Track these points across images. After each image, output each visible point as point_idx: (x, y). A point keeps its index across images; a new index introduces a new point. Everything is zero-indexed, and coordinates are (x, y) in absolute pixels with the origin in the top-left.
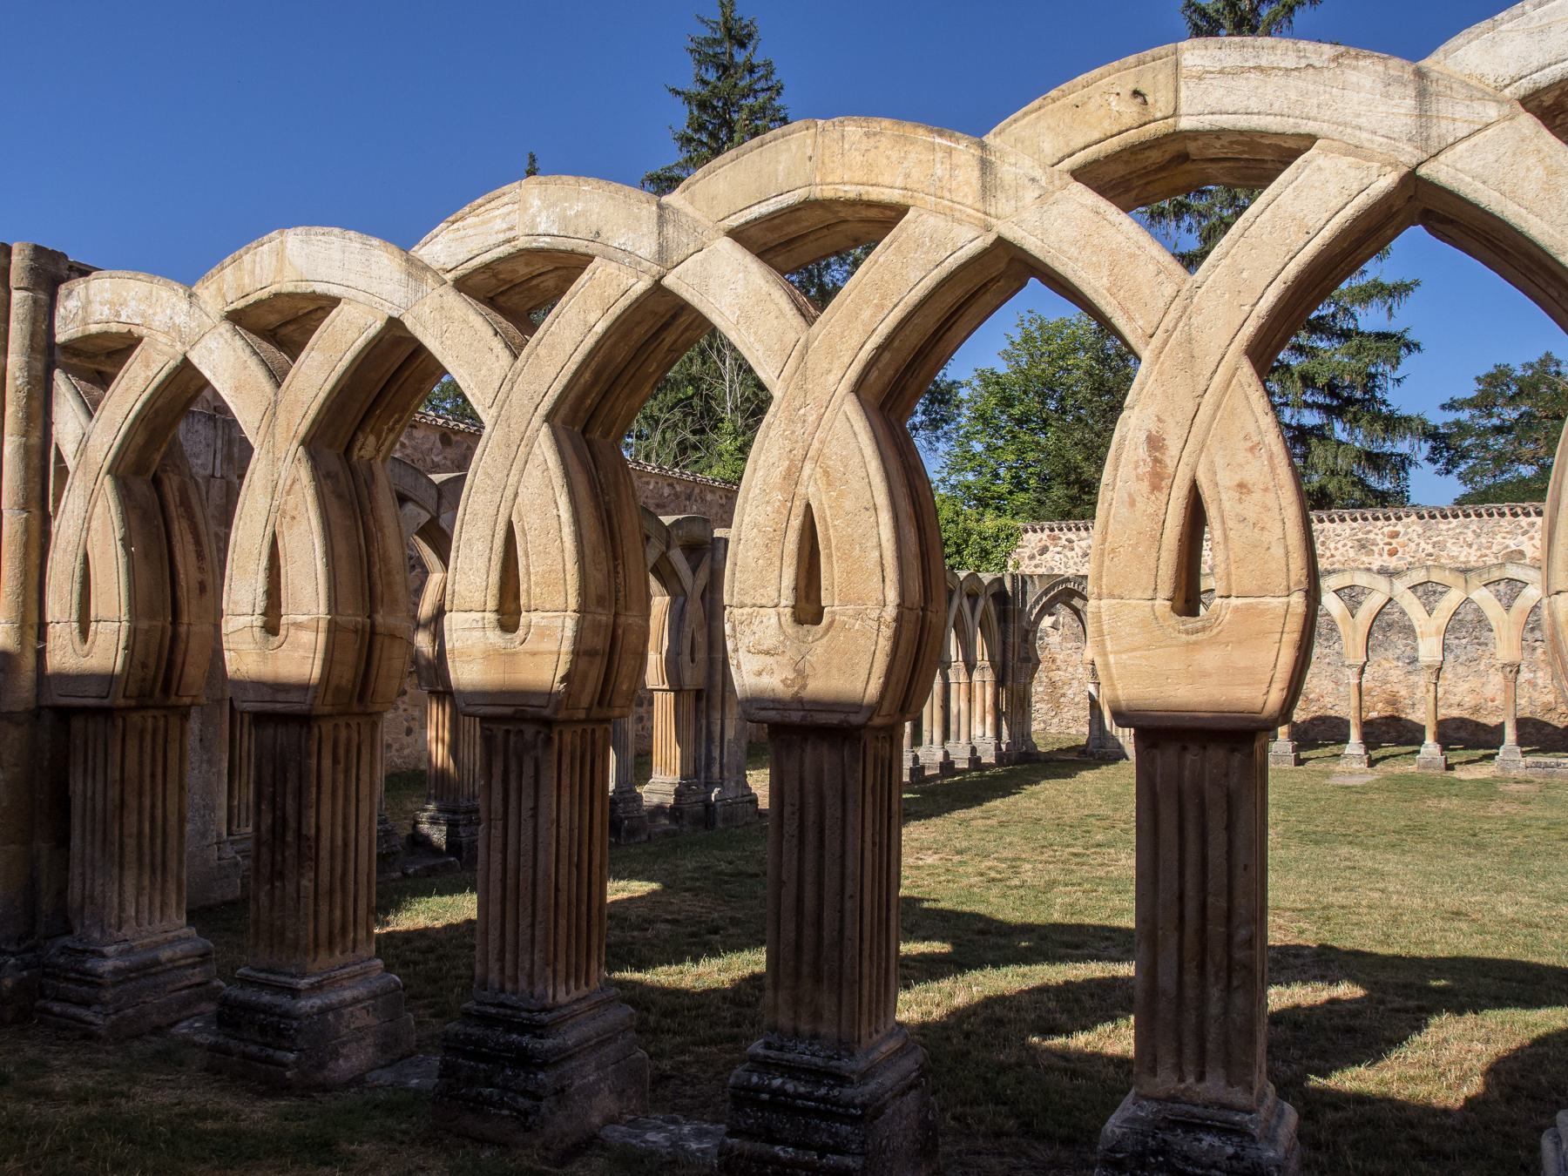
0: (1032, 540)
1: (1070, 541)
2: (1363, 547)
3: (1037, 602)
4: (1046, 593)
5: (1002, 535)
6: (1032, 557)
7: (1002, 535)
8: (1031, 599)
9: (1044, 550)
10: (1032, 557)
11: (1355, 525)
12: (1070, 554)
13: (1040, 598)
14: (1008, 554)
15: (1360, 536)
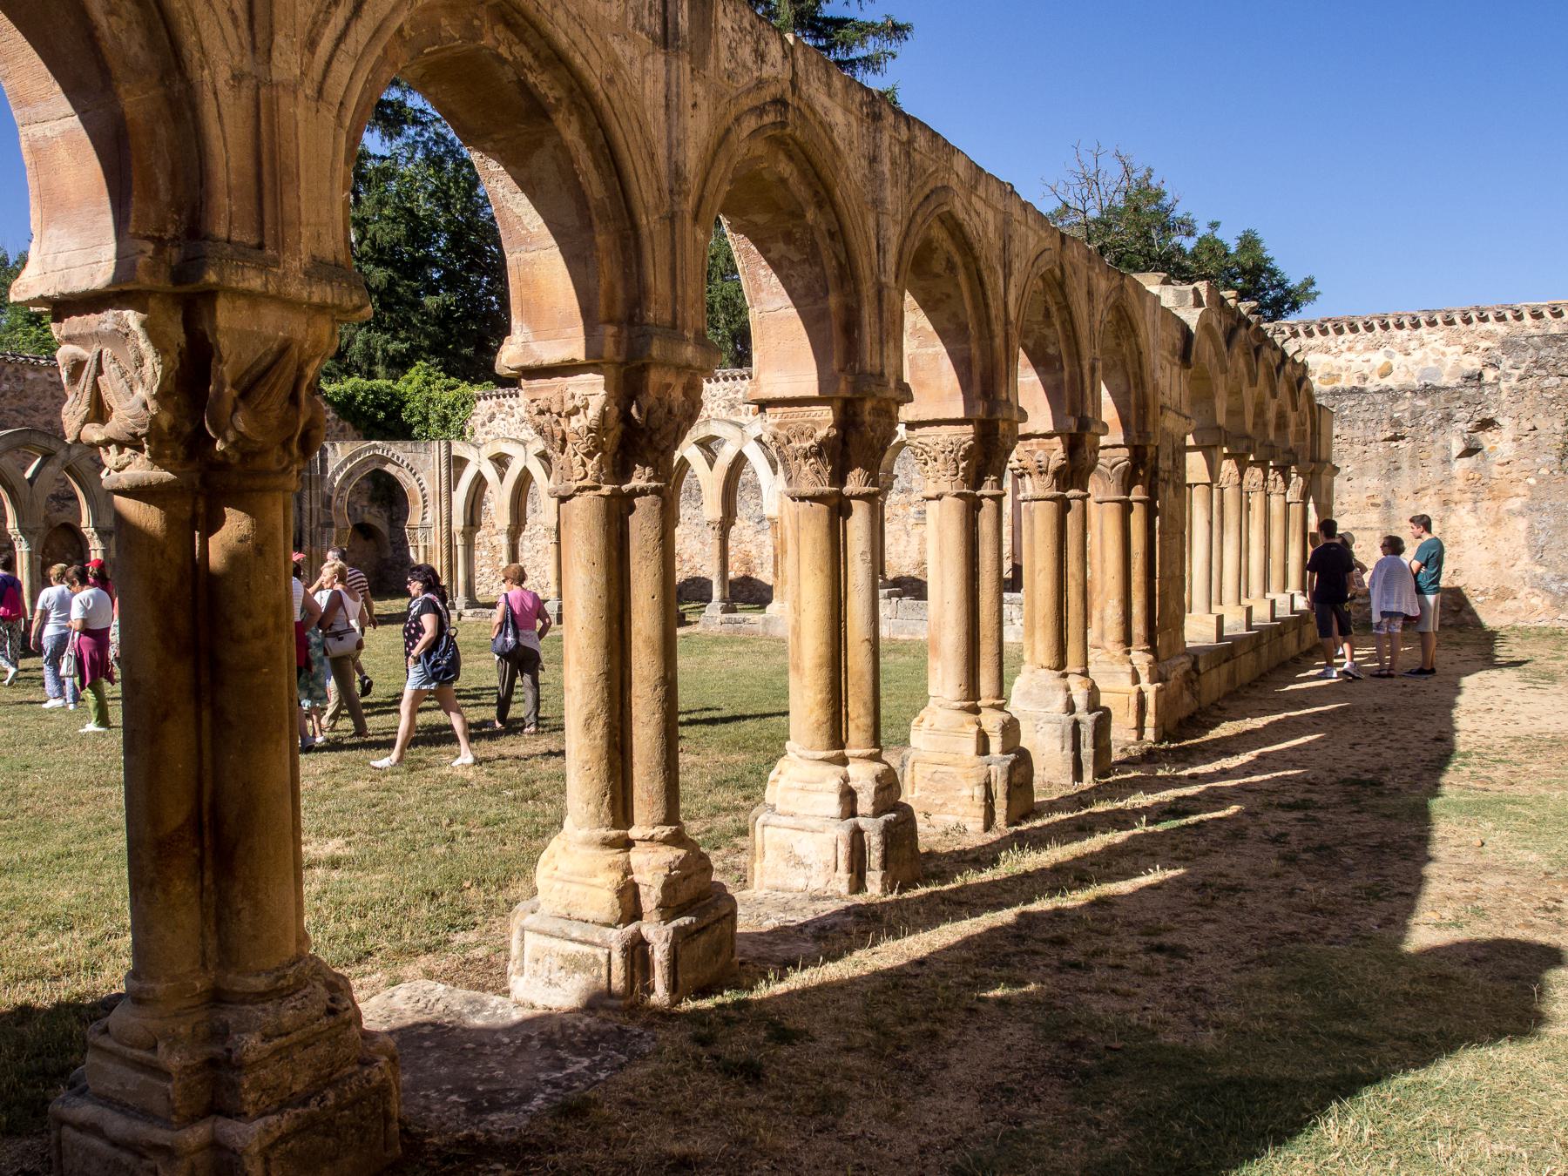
0: (484, 407)
1: (511, 407)
2: (733, 406)
3: (340, 468)
4: (350, 459)
5: (458, 404)
6: (483, 425)
7: (458, 404)
8: (332, 466)
9: (492, 418)
10: (483, 425)
11: (726, 384)
12: (512, 420)
13: (344, 464)
14: (464, 422)
15: (731, 396)
